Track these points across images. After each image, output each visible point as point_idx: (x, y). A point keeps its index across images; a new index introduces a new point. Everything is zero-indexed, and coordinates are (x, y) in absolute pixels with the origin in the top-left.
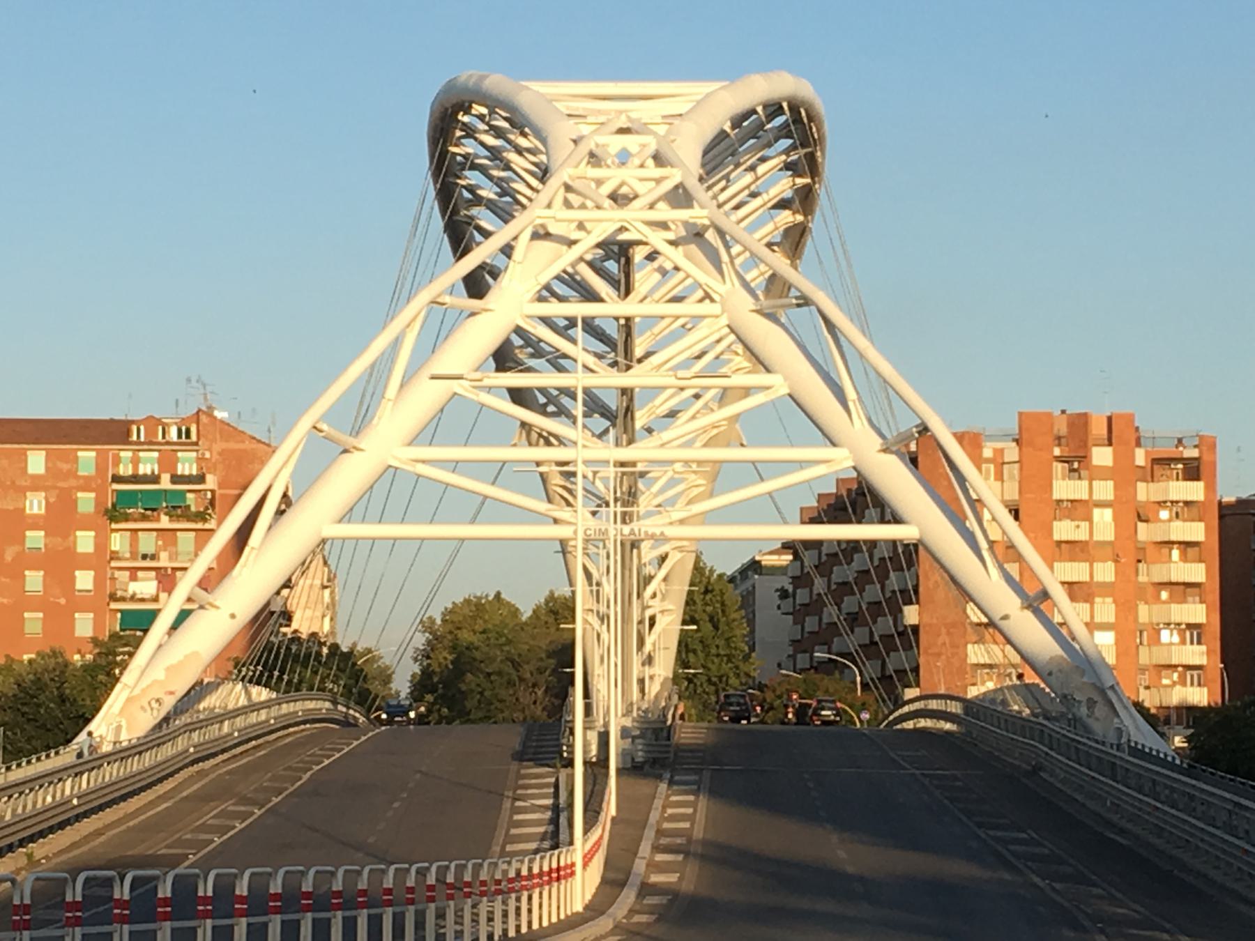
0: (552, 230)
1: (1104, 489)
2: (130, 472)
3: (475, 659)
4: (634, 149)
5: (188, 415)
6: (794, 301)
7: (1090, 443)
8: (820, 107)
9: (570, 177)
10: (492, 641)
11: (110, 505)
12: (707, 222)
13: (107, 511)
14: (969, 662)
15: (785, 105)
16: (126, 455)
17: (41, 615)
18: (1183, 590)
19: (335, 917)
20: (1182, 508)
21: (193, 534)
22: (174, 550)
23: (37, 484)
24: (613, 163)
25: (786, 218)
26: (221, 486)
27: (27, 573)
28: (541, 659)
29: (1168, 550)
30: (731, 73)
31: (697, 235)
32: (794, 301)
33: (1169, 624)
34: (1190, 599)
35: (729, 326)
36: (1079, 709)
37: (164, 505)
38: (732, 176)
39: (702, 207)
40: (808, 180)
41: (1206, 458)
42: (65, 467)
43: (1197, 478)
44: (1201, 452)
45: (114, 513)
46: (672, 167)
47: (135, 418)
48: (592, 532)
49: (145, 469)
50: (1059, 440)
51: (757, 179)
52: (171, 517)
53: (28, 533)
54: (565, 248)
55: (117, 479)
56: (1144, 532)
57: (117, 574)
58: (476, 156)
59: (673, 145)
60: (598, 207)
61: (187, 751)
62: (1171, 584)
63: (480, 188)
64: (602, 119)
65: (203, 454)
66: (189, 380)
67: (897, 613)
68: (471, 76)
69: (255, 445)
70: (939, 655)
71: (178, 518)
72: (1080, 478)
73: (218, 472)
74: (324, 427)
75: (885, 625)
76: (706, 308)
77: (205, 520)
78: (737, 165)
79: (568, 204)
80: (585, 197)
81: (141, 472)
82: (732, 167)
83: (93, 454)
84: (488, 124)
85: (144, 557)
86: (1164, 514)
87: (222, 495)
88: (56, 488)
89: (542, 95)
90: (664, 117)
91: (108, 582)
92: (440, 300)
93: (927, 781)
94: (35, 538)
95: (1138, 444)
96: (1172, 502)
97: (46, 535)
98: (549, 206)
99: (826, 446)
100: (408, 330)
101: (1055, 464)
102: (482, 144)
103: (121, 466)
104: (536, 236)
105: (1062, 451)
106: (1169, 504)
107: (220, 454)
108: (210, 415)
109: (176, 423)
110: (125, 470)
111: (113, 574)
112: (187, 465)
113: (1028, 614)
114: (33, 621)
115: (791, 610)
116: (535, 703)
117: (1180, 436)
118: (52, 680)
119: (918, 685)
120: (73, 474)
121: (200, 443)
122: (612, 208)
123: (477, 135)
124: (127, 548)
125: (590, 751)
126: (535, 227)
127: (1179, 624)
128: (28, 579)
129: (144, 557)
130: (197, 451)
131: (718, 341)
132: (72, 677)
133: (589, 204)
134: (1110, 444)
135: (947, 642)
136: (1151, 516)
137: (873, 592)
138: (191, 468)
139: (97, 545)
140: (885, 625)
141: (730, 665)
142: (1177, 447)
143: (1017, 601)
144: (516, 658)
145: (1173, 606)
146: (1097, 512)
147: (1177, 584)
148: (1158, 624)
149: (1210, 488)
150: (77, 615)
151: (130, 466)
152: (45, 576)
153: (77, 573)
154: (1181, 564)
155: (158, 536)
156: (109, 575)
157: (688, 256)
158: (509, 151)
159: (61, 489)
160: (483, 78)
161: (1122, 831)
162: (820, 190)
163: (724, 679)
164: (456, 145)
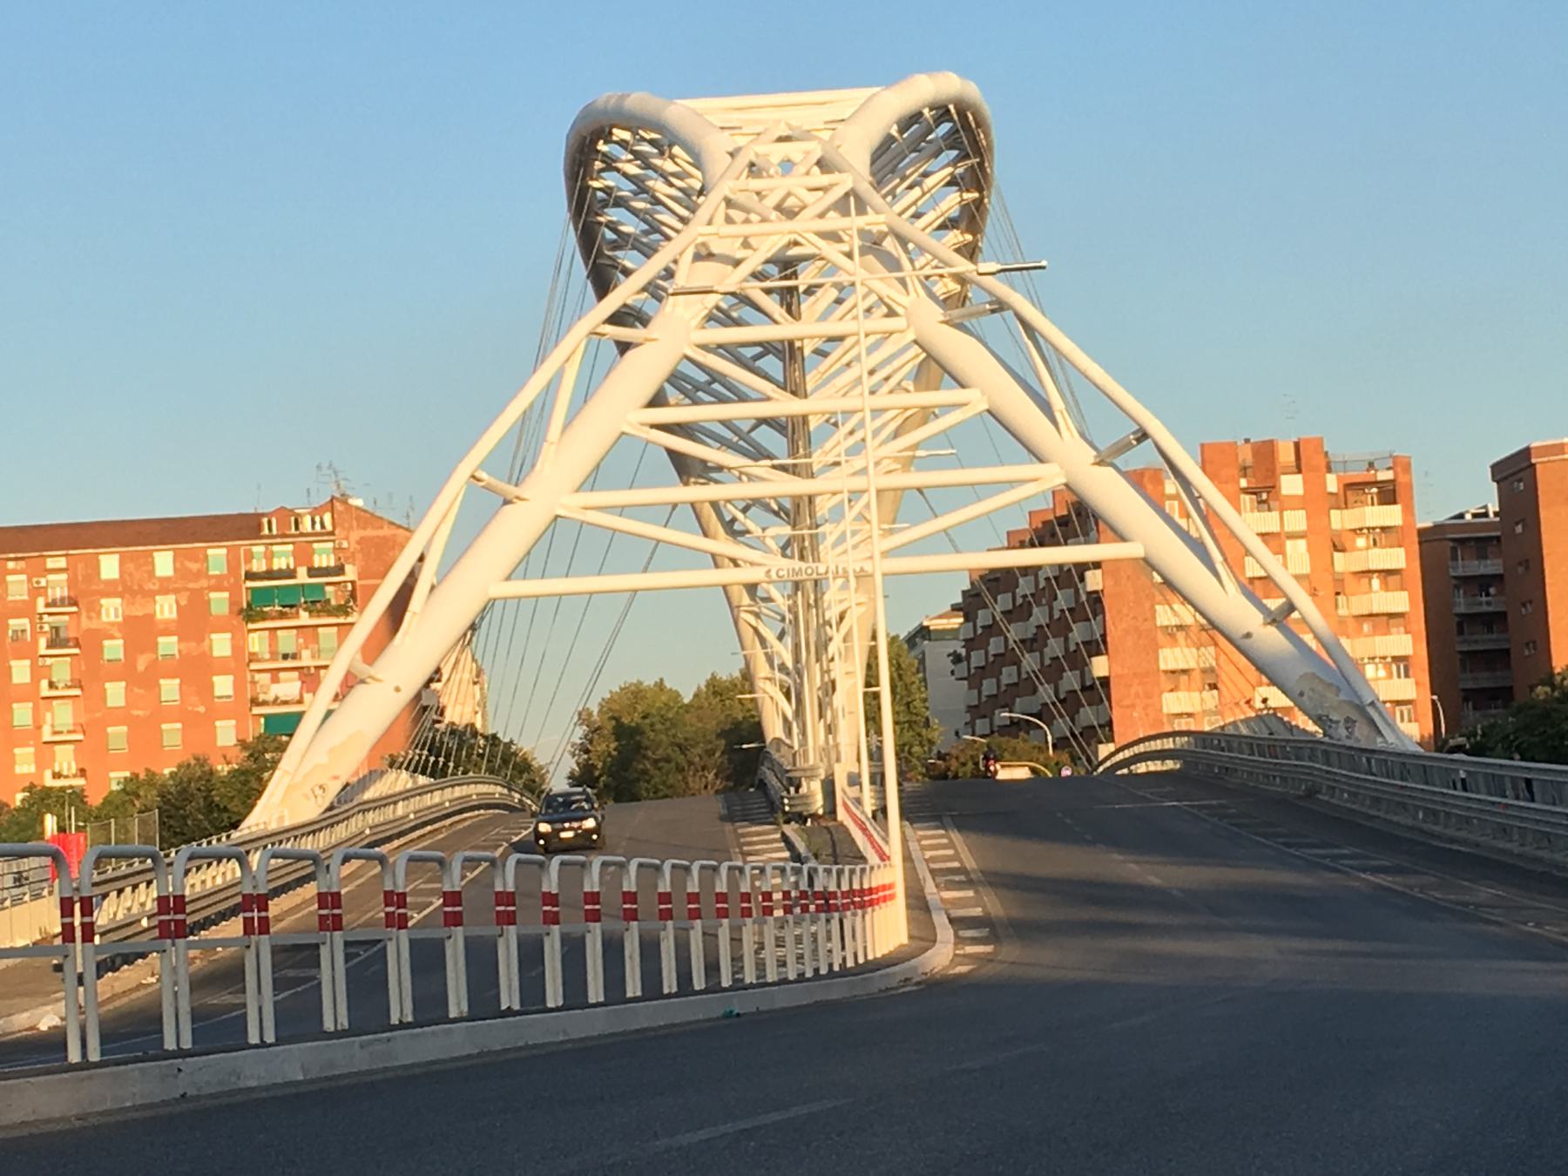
0: (715, 250)
1: (1296, 520)
2: (264, 568)
3: (639, 747)
4: (797, 157)
5: (322, 503)
6: (988, 307)
7: (1278, 470)
8: (987, 111)
9: (732, 190)
10: (658, 726)
11: (245, 605)
12: (885, 229)
13: (241, 611)
14: (1165, 710)
15: (951, 107)
16: (258, 550)
17: (179, 725)
18: (1387, 620)
19: (664, 929)
20: (1380, 534)
21: (335, 629)
23: (165, 587)
24: (777, 173)
25: (955, 237)
26: (360, 579)
27: (162, 682)
28: (710, 742)
29: (1366, 580)
30: (891, 77)
31: (872, 244)
32: (988, 307)
33: (1373, 658)
34: (1394, 630)
35: (915, 342)
36: (1336, 729)
37: (303, 600)
38: (899, 190)
39: (877, 212)
40: (976, 195)
41: (1402, 479)
42: (194, 566)
43: (1394, 502)
44: (1396, 474)
45: (251, 613)
46: (840, 171)
47: (265, 511)
48: (785, 573)
49: (280, 563)
50: (1244, 471)
51: (924, 194)
52: (310, 612)
53: (161, 640)
54: (730, 268)
55: (250, 576)
56: (1341, 562)
57: (258, 677)
58: (620, 189)
59: (840, 150)
60: (764, 220)
61: (362, 832)
62: (1371, 615)
63: (623, 224)
64: (760, 129)
65: (340, 544)
66: (319, 467)
67: (1081, 666)
68: (610, 97)
69: (394, 531)
70: (1133, 706)
71: (318, 613)
72: (1269, 510)
73: (357, 562)
74: (483, 475)
75: (1071, 680)
76: (891, 323)
77: (347, 614)
78: (903, 179)
79: (729, 220)
80: (747, 210)
81: (275, 567)
82: (898, 180)
83: (224, 551)
84: (632, 152)
85: (285, 657)
86: (1361, 542)
87: (361, 586)
89: (694, 111)
90: (826, 123)
91: (249, 685)
92: (599, 330)
93: (1195, 811)
94: (168, 645)
95: (1329, 470)
96: (1368, 529)
97: (180, 640)
98: (710, 223)
99: (1031, 462)
100: (567, 365)
101: (1242, 496)
102: (625, 175)
103: (254, 561)
104: (698, 257)
105: (1248, 482)
106: (1365, 531)
107: (358, 543)
108: (345, 502)
109: (309, 513)
110: (258, 566)
111: (253, 677)
112: (324, 556)
113: (1272, 630)
114: (172, 733)
115: (966, 675)
116: (706, 787)
117: (1371, 458)
118: (199, 790)
119: (1113, 741)
120: (202, 574)
121: (337, 532)
122: (780, 220)
123: (620, 165)
124: (266, 648)
125: (814, 803)
126: (696, 246)
127: (1384, 658)
128: (163, 689)
129: (285, 657)
130: (333, 541)
131: (887, 379)
132: (218, 785)
133: (753, 217)
134: (1299, 471)
135: (1141, 693)
136: (1347, 546)
137: (1054, 647)
138: (328, 560)
139: (234, 648)
140: (1071, 680)
141: (911, 733)
142: (1368, 470)
143: (1259, 617)
144: (682, 741)
145: (1378, 639)
146: (1289, 544)
147: (1383, 615)
148: (1362, 659)
149: (1408, 511)
150: (218, 723)
151: (264, 561)
152: (181, 685)
153: (216, 679)
154: (1383, 593)
155: (297, 635)
156: (249, 679)
157: (863, 266)
158: (651, 179)
159: (188, 589)
160: (623, 97)
161: (1452, 840)
162: (992, 202)
163: (906, 748)
164: (596, 179)
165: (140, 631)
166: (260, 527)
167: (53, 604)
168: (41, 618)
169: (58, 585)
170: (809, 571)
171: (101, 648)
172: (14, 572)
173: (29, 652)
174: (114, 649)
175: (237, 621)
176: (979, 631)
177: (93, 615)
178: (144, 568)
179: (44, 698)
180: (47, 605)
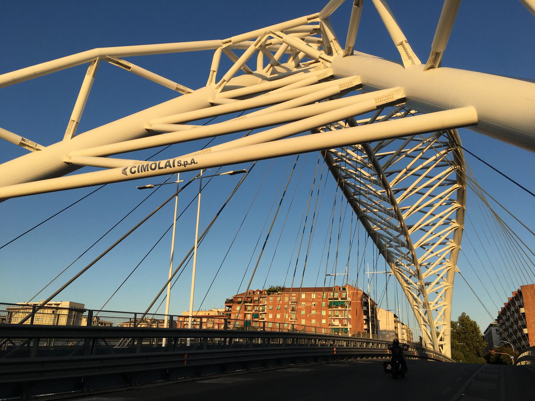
45: (330, 306)
48: (136, 169)
55: (330, 299)
67: (521, 331)
88: (318, 301)
129: (336, 316)
159: (319, 301)
163: (478, 347)
165: (309, 309)
167: (293, 302)
169: (294, 298)
170: (153, 167)
172: (286, 296)
174: (303, 312)
175: (327, 308)
176: (501, 324)
180: (291, 303)
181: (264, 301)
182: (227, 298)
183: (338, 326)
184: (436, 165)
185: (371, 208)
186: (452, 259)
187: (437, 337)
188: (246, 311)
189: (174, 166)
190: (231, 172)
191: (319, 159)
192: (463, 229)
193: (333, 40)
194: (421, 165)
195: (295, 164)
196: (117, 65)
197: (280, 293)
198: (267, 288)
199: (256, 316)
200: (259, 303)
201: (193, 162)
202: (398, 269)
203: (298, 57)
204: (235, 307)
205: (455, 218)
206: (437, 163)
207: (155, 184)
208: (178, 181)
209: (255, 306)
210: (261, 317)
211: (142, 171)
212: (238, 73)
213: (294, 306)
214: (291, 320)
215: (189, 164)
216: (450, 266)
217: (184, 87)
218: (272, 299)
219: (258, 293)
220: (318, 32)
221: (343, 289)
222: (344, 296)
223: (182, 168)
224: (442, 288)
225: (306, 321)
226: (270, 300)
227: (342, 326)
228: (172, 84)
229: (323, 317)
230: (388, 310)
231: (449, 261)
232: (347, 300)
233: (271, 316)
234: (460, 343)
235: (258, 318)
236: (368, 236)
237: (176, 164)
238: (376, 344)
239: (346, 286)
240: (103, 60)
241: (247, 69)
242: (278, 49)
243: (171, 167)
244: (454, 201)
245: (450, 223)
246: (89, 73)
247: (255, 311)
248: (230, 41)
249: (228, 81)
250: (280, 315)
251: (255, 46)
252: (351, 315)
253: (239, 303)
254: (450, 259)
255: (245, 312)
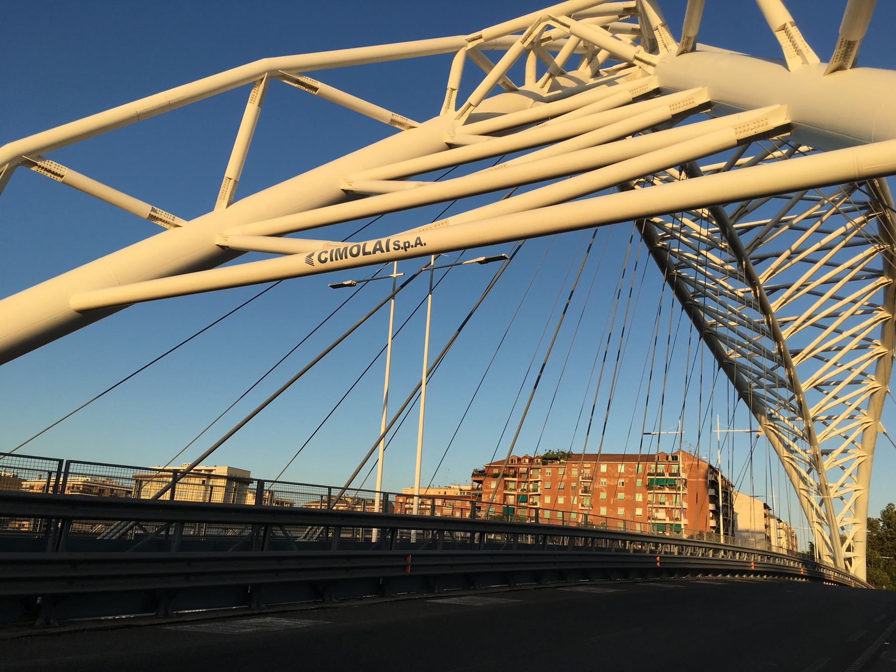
22: (672, 501)
26: (689, 477)
45: (649, 487)
48: (328, 256)
52: (669, 488)
55: (650, 474)
88: (628, 477)
107: (687, 466)
110: (653, 471)
129: (661, 503)
139: (643, 499)
159: (629, 477)
165: (613, 491)
166: (654, 459)
167: (585, 478)
168: (581, 483)
170: (355, 251)
171: (599, 495)
173: (576, 494)
174: (603, 496)
177: (598, 483)
178: (615, 469)
179: (581, 509)
180: (582, 479)
181: (537, 475)
182: (476, 468)
183: (664, 520)
184: (846, 243)
185: (725, 320)
186: (872, 409)
187: (842, 546)
188: (506, 489)
189: (388, 250)
190: (482, 259)
191: (632, 236)
192: (893, 357)
193: (659, 27)
194: (818, 243)
195: (591, 245)
196: (296, 85)
197: (564, 461)
198: (542, 453)
199: (522, 498)
200: (528, 477)
201: (418, 242)
202: (773, 425)
203: (597, 59)
204: (488, 483)
205: (880, 338)
206: (848, 239)
207: (358, 280)
208: (395, 275)
209: (520, 482)
210: (531, 500)
211: (337, 259)
212: (494, 91)
213: (588, 485)
214: (583, 508)
215: (412, 246)
216: (867, 423)
217: (404, 117)
218: (550, 471)
219: (527, 460)
220: (632, 14)
221: (673, 457)
222: (674, 471)
223: (401, 252)
224: (853, 460)
225: (607, 510)
226: (547, 473)
227: (670, 520)
228: (384, 114)
229: (637, 505)
230: (753, 497)
231: (866, 414)
232: (679, 478)
233: (548, 500)
234: (883, 555)
235: (527, 502)
236: (719, 369)
237: (391, 246)
238: (731, 552)
239: (678, 452)
240: (275, 78)
241: (508, 83)
242: (561, 47)
243: (383, 251)
244: (879, 306)
245: (869, 346)
246: (252, 100)
247: (521, 490)
248: (480, 37)
249: (476, 106)
250: (563, 499)
251: (523, 44)
252: (686, 502)
253: (496, 476)
254: (868, 408)
255: (504, 492)
